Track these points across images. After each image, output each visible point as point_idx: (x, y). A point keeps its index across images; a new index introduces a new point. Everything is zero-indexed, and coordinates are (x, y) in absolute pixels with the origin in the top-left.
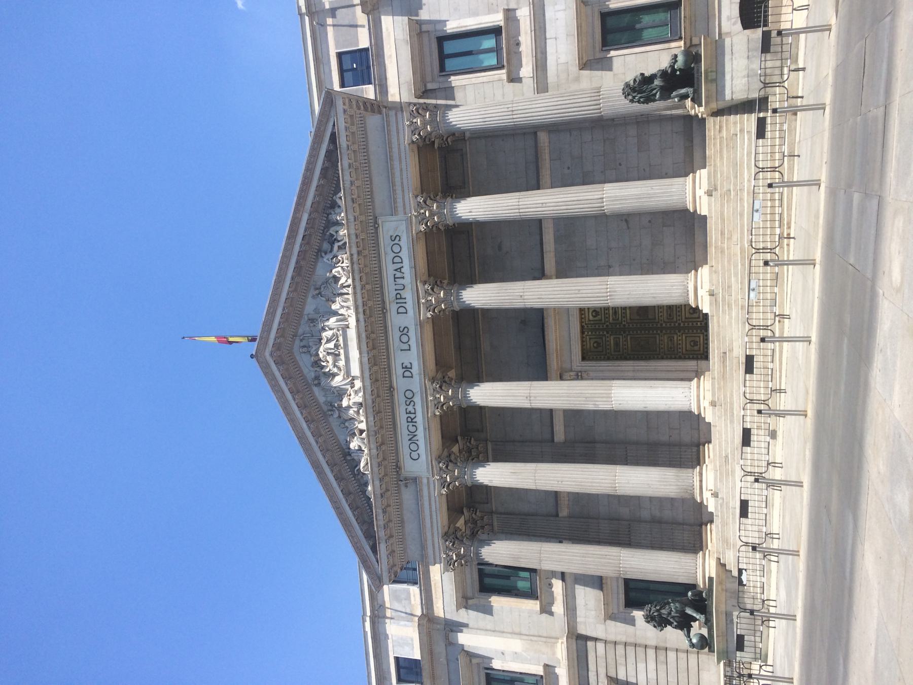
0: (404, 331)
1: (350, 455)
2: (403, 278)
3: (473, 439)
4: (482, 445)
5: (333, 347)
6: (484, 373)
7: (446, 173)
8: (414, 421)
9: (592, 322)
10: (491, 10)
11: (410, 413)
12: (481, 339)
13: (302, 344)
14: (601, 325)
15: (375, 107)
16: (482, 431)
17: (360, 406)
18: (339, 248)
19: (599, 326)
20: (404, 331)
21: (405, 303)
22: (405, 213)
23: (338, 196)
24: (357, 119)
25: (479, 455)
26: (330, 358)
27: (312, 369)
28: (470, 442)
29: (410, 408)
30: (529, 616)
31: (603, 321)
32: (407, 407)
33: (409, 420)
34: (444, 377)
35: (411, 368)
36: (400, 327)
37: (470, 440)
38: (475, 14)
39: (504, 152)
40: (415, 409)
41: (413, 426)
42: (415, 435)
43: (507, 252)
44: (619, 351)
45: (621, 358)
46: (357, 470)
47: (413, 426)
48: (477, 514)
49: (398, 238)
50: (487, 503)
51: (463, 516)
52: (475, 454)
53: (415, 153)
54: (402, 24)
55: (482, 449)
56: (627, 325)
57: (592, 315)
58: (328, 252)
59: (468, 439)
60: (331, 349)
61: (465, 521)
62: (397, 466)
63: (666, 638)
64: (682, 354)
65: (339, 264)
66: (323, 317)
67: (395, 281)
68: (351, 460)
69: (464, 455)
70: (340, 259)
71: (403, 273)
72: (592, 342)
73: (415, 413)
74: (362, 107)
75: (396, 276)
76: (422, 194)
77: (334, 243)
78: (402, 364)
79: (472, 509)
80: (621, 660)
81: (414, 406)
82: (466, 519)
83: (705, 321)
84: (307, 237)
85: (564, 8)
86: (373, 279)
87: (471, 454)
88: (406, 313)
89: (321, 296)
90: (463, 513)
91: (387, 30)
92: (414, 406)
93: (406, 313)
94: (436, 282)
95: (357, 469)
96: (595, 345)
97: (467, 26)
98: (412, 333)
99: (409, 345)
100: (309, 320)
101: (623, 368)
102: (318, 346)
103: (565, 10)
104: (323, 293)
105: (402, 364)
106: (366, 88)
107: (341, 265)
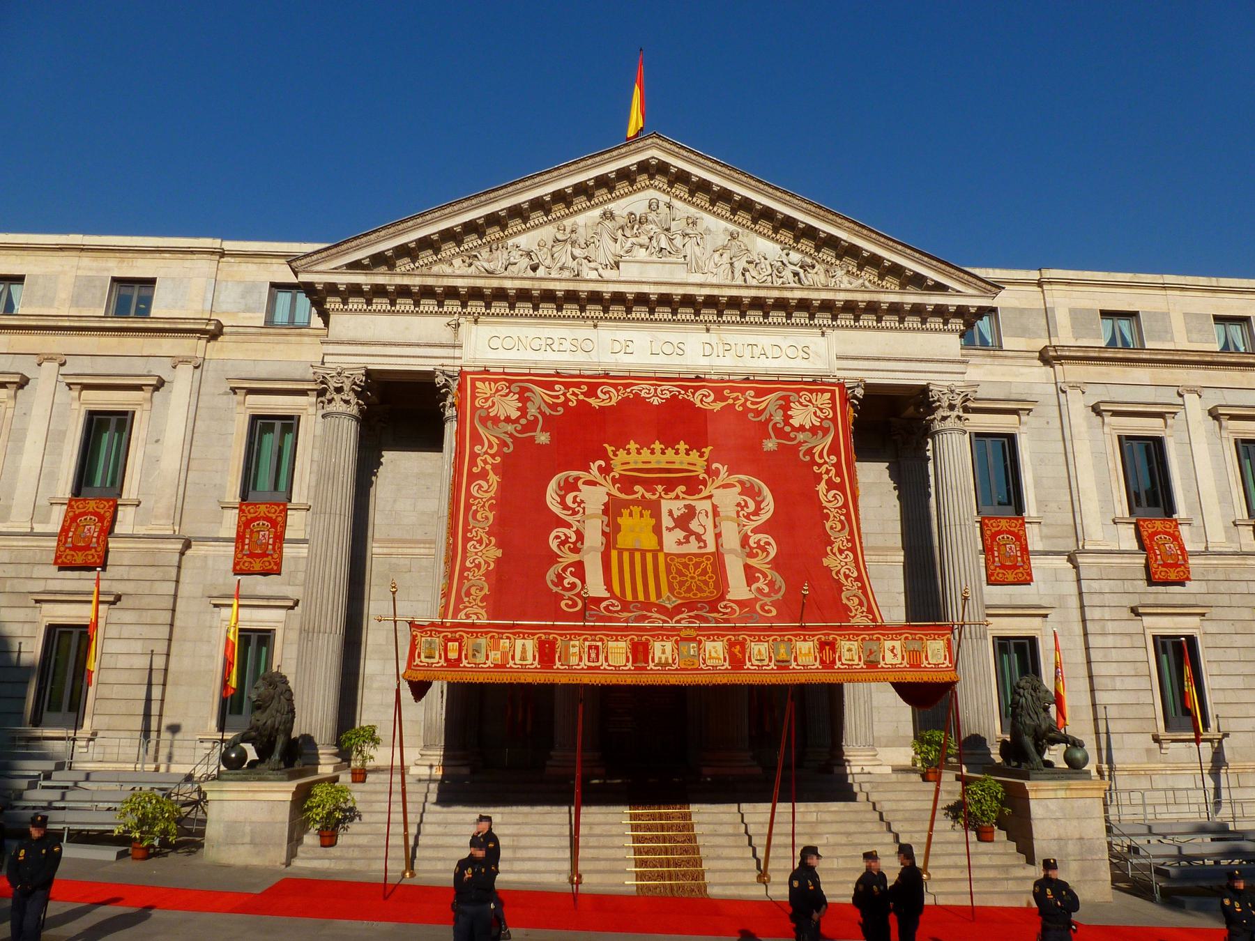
10: (1041, 503)
13: (661, 204)
22: (838, 369)
23: (867, 283)
26: (644, 239)
27: (627, 213)
33: (550, 342)
38: (1037, 483)
46: (476, 256)
49: (806, 356)
63: (181, 685)
65: (775, 271)
67: (748, 345)
77: (801, 267)
80: (147, 617)
85: (1041, 593)
91: (1022, 374)
97: (1024, 472)
103: (1039, 594)
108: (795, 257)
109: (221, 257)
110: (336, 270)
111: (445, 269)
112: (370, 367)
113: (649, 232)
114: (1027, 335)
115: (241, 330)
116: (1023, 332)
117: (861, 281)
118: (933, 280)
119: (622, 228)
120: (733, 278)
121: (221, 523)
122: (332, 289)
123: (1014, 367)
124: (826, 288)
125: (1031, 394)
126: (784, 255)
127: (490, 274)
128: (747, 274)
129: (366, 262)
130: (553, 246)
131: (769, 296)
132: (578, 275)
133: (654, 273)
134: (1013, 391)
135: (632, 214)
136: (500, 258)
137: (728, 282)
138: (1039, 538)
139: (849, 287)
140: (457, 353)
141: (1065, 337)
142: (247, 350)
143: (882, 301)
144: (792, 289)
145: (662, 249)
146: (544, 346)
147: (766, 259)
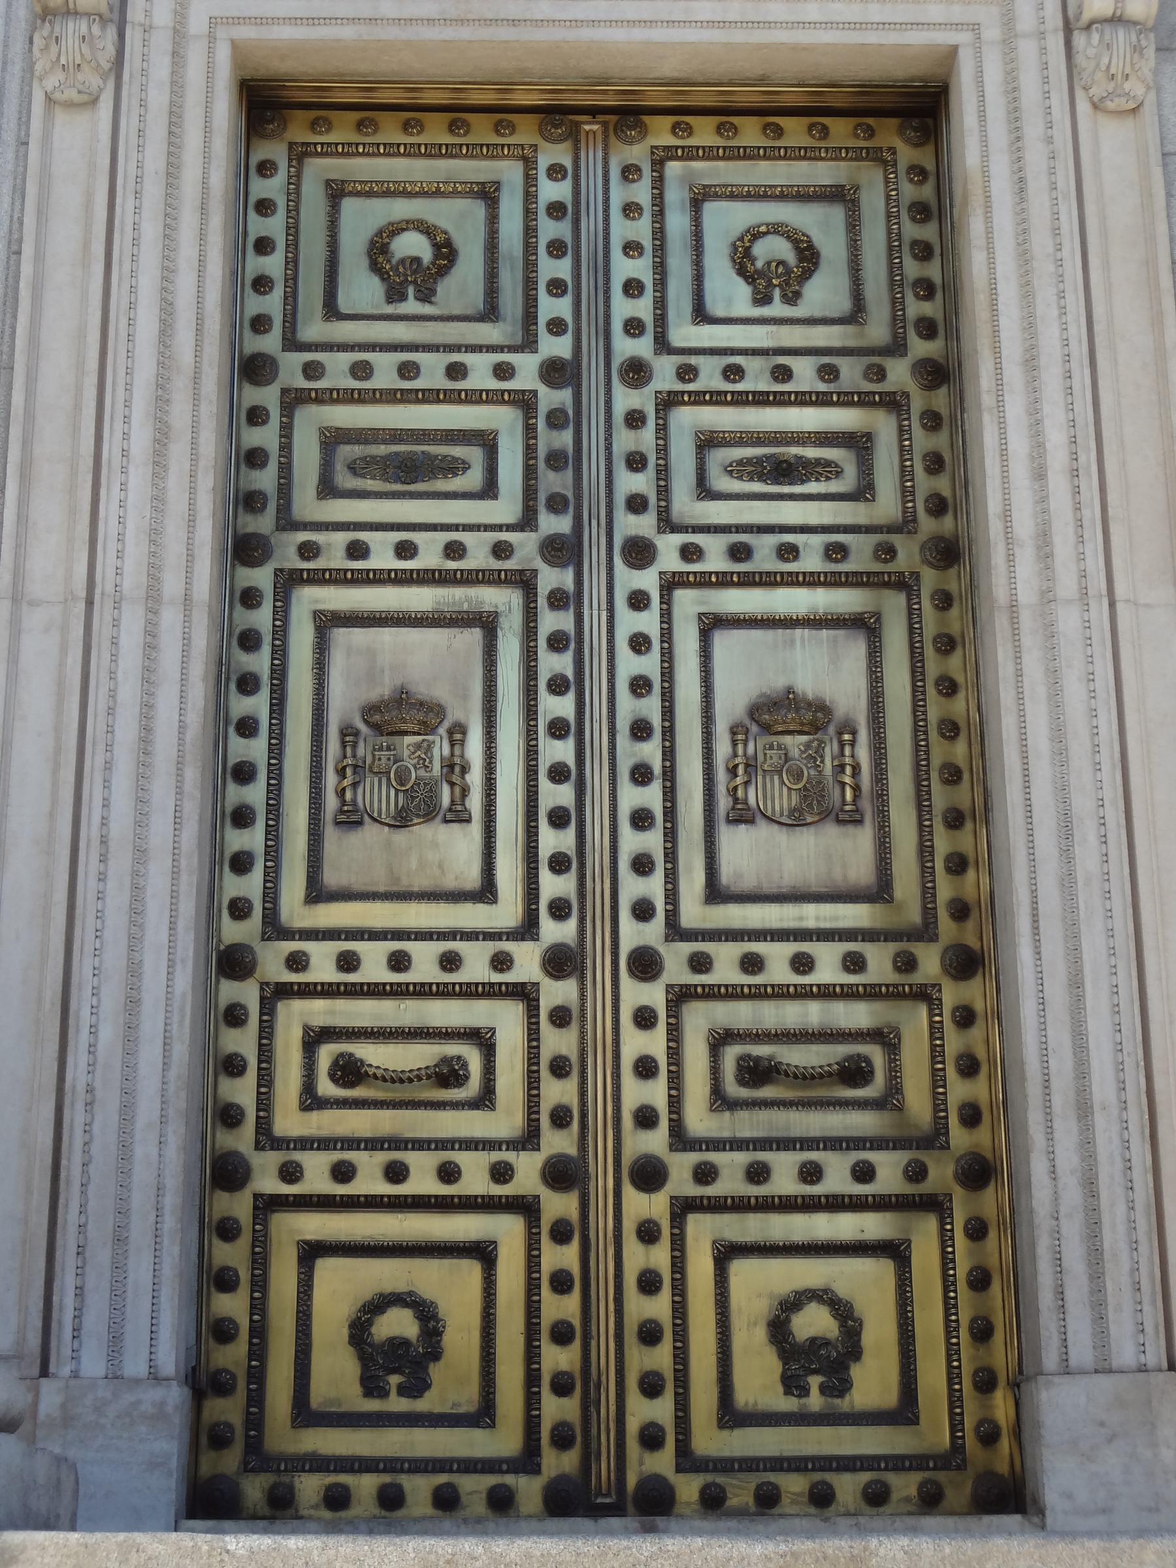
9: (677, 222)
14: (643, 308)
19: (633, 288)
31: (684, 333)
44: (328, 489)
45: (251, 501)
56: (648, 580)
57: (755, 234)
64: (268, 1205)
72: (439, 212)
83: (688, 1488)
96: (412, 245)
101: (139, 477)
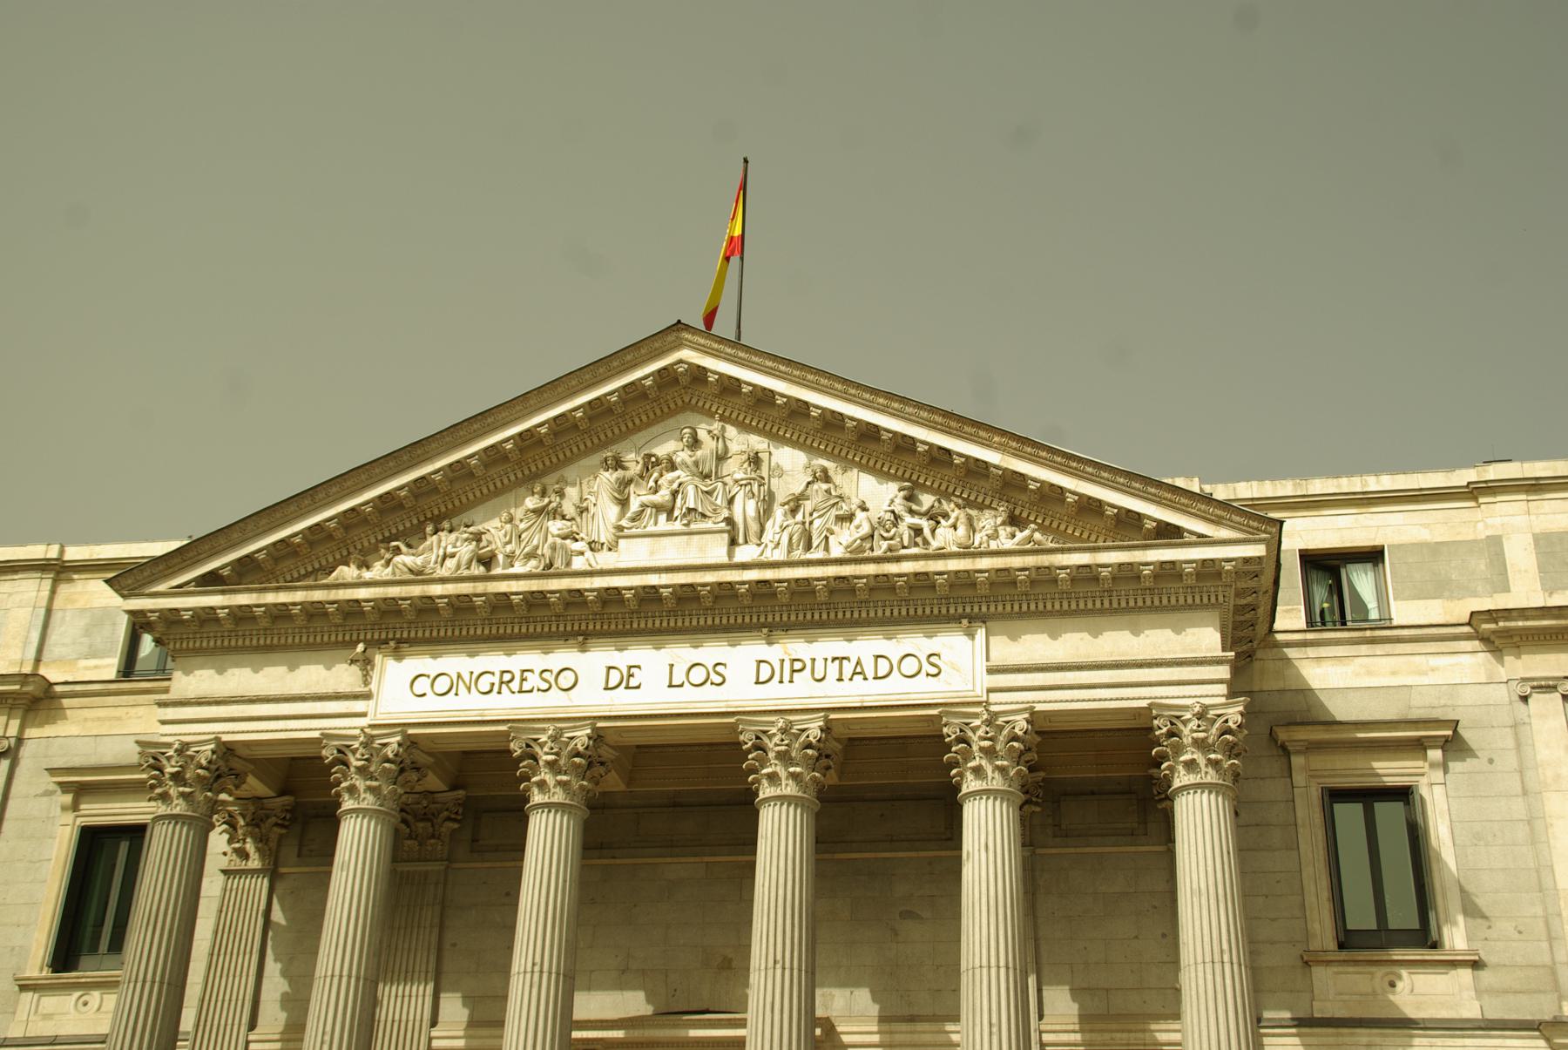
0: (716, 676)
1: (435, 533)
2: (840, 680)
3: (456, 826)
4: (439, 848)
5: (692, 506)
6: (612, 861)
7: (1093, 793)
8: (504, 686)
11: (523, 680)
12: (692, 859)
13: (702, 434)
15: (1247, 632)
16: (472, 851)
17: (548, 561)
18: (918, 531)
20: (716, 676)
21: (781, 682)
22: (990, 691)
23: (1037, 536)
24: (1212, 589)
25: (415, 839)
26: (663, 496)
28: (448, 819)
29: (533, 681)
30: (13, 949)
32: (537, 672)
33: (507, 677)
34: (602, 764)
35: (627, 687)
36: (725, 665)
37: (455, 820)
39: (1136, 937)
40: (531, 691)
41: (493, 684)
42: (469, 689)
43: (896, 934)
46: (398, 548)
47: (493, 684)
48: (275, 829)
49: (934, 671)
50: (299, 855)
51: (269, 793)
52: (421, 831)
53: (1134, 722)
54: (1444, 706)
55: (429, 848)
58: (911, 504)
59: (456, 813)
60: (684, 499)
61: (260, 798)
62: (400, 641)
66: (760, 486)
67: (834, 659)
68: (425, 533)
69: (419, 803)
70: (892, 533)
71: (851, 679)
73: (520, 691)
74: (1243, 602)
75: (845, 662)
76: (1037, 733)
78: (639, 667)
79: (288, 817)
81: (539, 690)
82: (265, 801)
84: (946, 457)
86: (840, 606)
87: (422, 820)
88: (756, 683)
89: (809, 483)
90: (282, 793)
92: (539, 690)
93: (757, 683)
94: (827, 756)
95: (403, 548)
98: (709, 692)
99: (681, 686)
100: (757, 453)
102: (694, 469)
104: (816, 486)
105: (639, 667)
106: (1300, 611)
107: (876, 533)
108: (927, 500)
109: (58, 573)
110: (179, 590)
111: (348, 572)
112: (225, 738)
113: (672, 482)
114: (1446, 594)
115: (78, 688)
116: (1438, 589)
117: (1027, 532)
118: (1155, 520)
119: (631, 481)
120: (808, 547)
121: (14, 1013)
122: (171, 618)
123: (1418, 657)
124: (967, 552)
125: (1454, 707)
126: (899, 501)
127: (418, 575)
128: (831, 538)
129: (226, 572)
130: (521, 521)
131: (858, 573)
132: (551, 565)
133: (674, 552)
134: (1414, 703)
135: (654, 456)
136: (435, 550)
137: (798, 554)
138: (1473, 993)
139: (1009, 544)
140: (359, 706)
141: (1526, 591)
142: (86, 720)
143: (1057, 564)
144: (898, 559)
145: (690, 510)
146: (496, 688)
147: (864, 509)
